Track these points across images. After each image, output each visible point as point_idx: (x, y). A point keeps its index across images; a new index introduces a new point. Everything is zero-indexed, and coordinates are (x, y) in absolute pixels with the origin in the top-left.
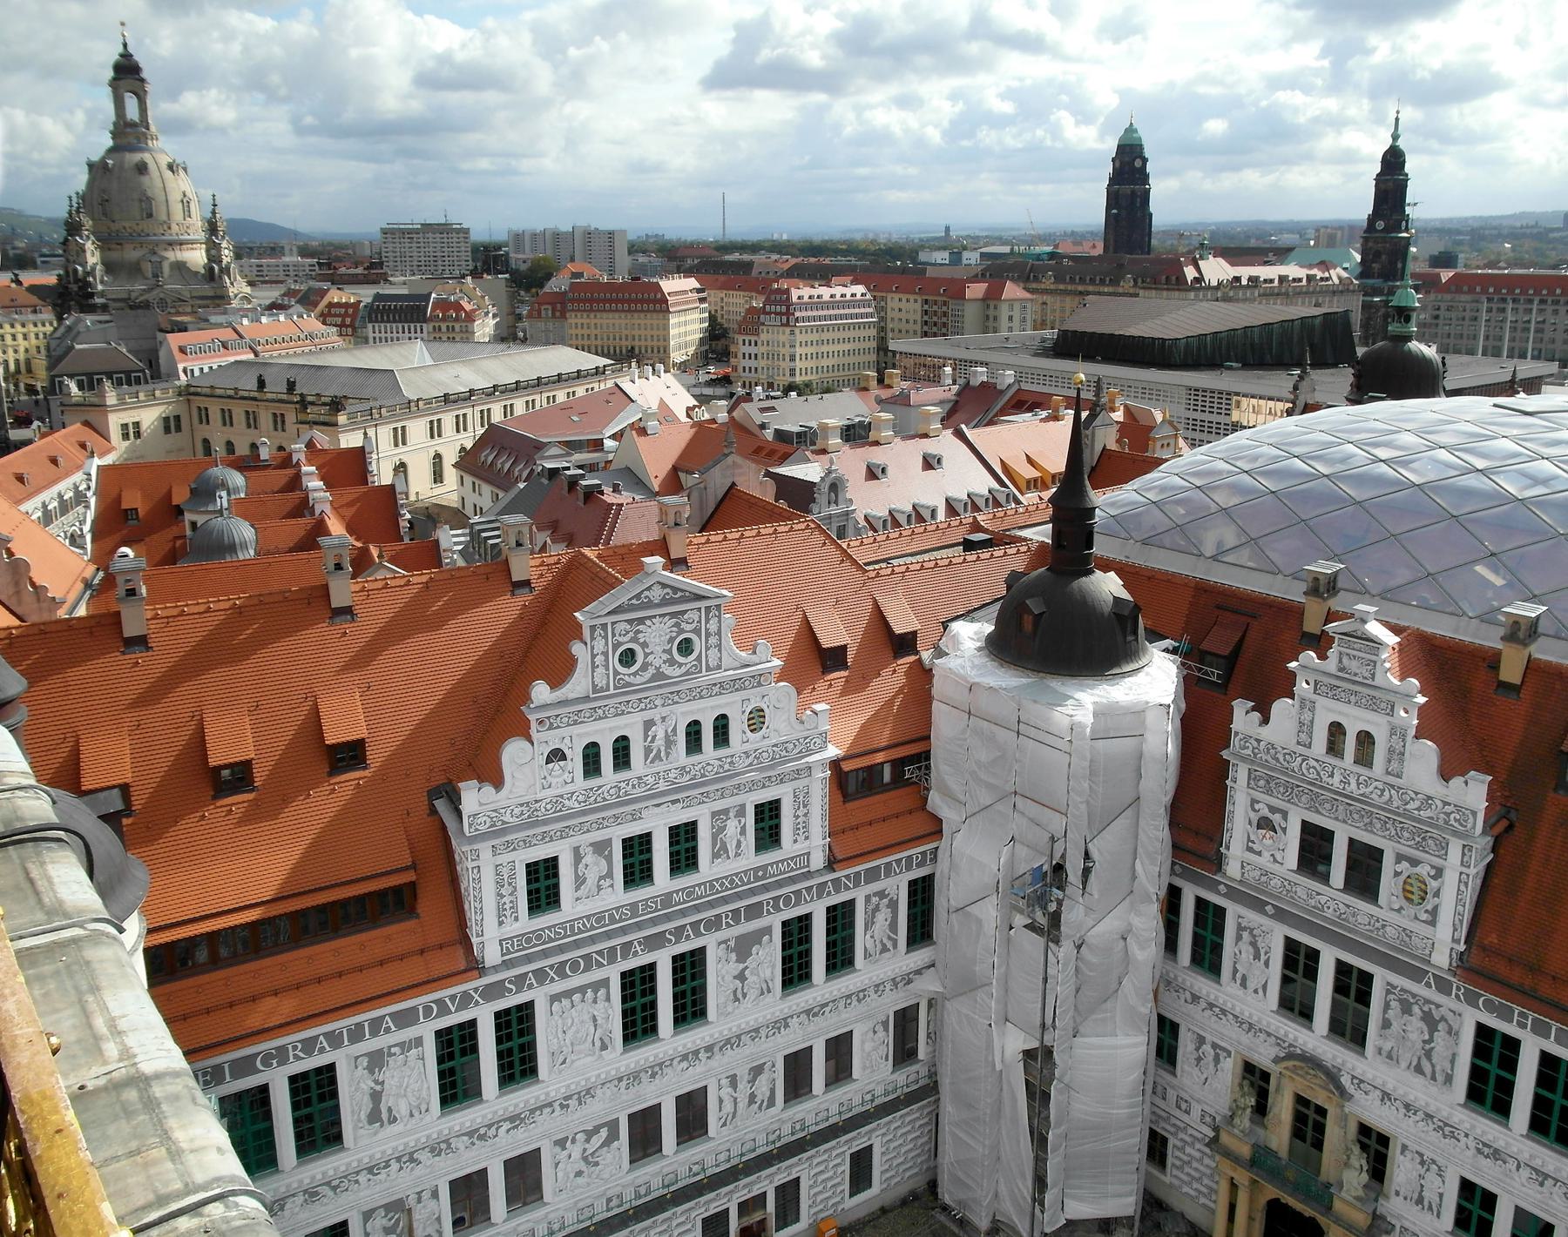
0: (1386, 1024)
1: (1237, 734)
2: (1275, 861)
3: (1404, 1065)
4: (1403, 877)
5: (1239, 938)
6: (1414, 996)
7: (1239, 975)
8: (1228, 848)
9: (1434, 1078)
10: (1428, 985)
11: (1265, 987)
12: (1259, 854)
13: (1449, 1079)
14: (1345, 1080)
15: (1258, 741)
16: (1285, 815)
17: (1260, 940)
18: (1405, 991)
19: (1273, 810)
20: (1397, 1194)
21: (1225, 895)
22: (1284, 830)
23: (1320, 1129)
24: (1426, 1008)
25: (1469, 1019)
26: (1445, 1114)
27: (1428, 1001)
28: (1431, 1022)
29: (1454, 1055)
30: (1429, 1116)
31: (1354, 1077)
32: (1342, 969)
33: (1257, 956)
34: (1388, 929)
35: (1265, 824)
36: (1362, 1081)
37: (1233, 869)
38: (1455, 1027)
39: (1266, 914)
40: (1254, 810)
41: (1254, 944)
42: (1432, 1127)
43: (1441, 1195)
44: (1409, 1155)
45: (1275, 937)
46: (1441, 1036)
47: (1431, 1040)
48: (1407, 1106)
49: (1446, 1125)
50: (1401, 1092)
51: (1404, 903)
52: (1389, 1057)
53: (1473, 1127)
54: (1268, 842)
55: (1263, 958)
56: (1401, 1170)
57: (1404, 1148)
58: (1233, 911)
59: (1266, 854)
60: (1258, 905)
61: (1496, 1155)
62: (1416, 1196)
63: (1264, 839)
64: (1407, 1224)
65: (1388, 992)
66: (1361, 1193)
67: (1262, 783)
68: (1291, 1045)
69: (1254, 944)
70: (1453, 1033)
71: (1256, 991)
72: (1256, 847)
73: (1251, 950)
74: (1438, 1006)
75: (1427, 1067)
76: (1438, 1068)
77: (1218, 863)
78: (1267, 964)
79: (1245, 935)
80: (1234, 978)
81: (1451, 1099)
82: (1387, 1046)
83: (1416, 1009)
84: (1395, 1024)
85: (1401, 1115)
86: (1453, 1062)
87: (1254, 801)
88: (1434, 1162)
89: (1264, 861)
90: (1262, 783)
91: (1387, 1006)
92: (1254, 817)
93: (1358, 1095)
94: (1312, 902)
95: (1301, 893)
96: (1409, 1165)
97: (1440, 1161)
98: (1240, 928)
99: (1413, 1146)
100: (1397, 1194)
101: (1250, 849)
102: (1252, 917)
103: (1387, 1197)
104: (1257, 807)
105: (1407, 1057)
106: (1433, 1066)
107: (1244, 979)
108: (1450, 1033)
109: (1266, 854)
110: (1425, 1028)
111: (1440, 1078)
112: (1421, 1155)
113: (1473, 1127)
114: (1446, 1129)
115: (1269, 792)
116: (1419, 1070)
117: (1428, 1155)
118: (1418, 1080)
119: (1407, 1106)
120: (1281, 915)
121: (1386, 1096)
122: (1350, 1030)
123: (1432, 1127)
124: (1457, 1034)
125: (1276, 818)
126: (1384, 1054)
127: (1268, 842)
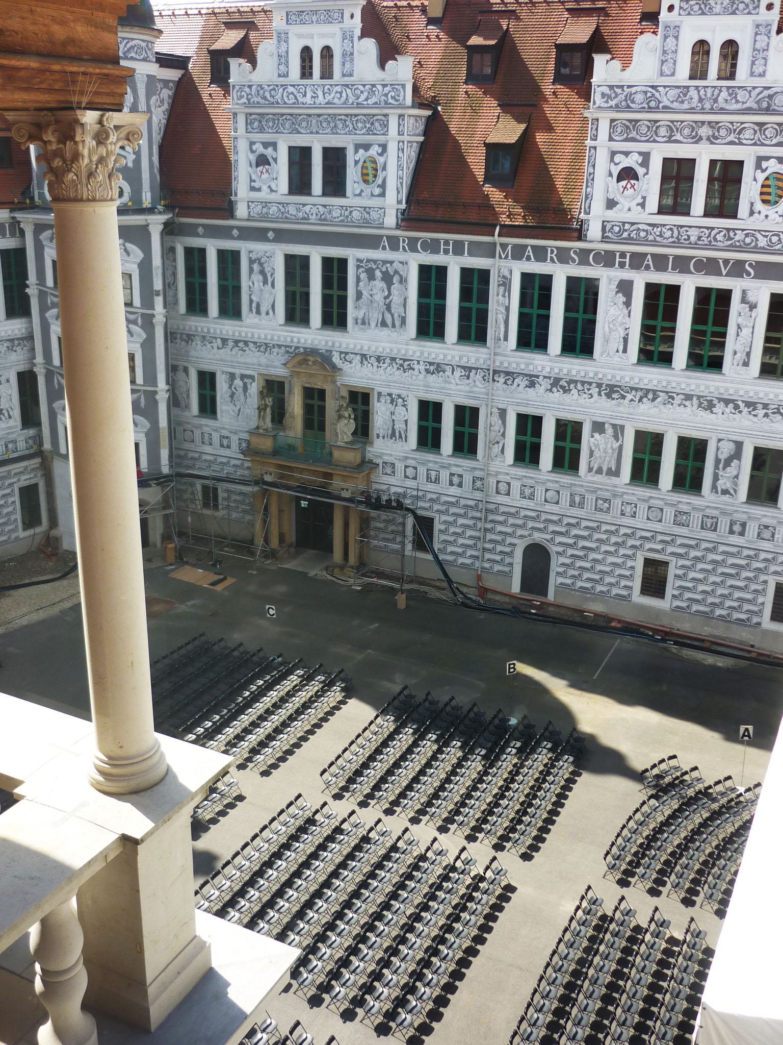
0: (359, 295)
1: (234, 86)
2: (272, 191)
3: (373, 324)
4: (361, 164)
5: (251, 271)
6: (375, 261)
7: (254, 305)
8: (236, 195)
9: (394, 326)
10: (384, 248)
11: (273, 306)
12: (259, 190)
13: (403, 321)
14: (336, 359)
15: (250, 87)
16: (274, 145)
17: (265, 265)
18: (368, 261)
19: (266, 145)
20: (378, 436)
21: (239, 238)
22: (275, 160)
23: (322, 410)
24: (384, 269)
25: (411, 263)
26: (403, 352)
27: (385, 262)
28: (388, 279)
29: (405, 299)
30: (393, 359)
31: (341, 353)
32: (327, 262)
33: (265, 282)
34: (354, 213)
35: (262, 161)
36: (347, 353)
37: (241, 211)
38: (404, 275)
39: (267, 240)
40: (252, 151)
41: (262, 272)
42: (396, 367)
43: (406, 421)
44: (382, 399)
45: (276, 256)
46: (396, 286)
47: (390, 294)
48: (379, 359)
49: (405, 360)
50: (373, 349)
51: (363, 186)
52: (363, 323)
53: (422, 353)
54: (265, 176)
55: (270, 280)
56: (380, 414)
57: (380, 394)
58: (246, 248)
59: (265, 188)
60: (259, 235)
61: (436, 368)
62: (390, 432)
63: (262, 177)
64: (386, 458)
65: (358, 267)
66: (350, 438)
67: (256, 124)
68: (297, 348)
69: (262, 272)
70: (403, 281)
71: (267, 313)
72: (256, 185)
73: (261, 277)
74: (391, 263)
75: (389, 321)
76: (396, 316)
77: (229, 211)
78: (273, 285)
79: (256, 267)
80: (251, 310)
81: (404, 340)
82: (361, 316)
83: (378, 274)
84: (364, 292)
85: (375, 367)
86: (405, 306)
87: (252, 143)
88: (399, 396)
89: (264, 195)
90: (256, 124)
91: (358, 280)
92: (253, 158)
93: (346, 367)
94: (300, 215)
95: (292, 210)
96: (383, 409)
97: (404, 393)
98: (251, 262)
99: (385, 391)
100: (378, 436)
101: (253, 189)
102: (259, 248)
103: (372, 443)
104: (254, 148)
105: (375, 317)
106: (392, 315)
107: (258, 305)
108: (401, 282)
109: (265, 188)
110: (385, 286)
111: (397, 323)
112: (390, 395)
113: (422, 353)
114: (405, 364)
115: (261, 130)
116: (384, 324)
117: (395, 392)
118: (385, 332)
119: (379, 359)
120: (282, 236)
121: (364, 357)
122: (335, 317)
123: (396, 367)
124: (406, 280)
125: (269, 152)
126: (360, 321)
127: (265, 176)
